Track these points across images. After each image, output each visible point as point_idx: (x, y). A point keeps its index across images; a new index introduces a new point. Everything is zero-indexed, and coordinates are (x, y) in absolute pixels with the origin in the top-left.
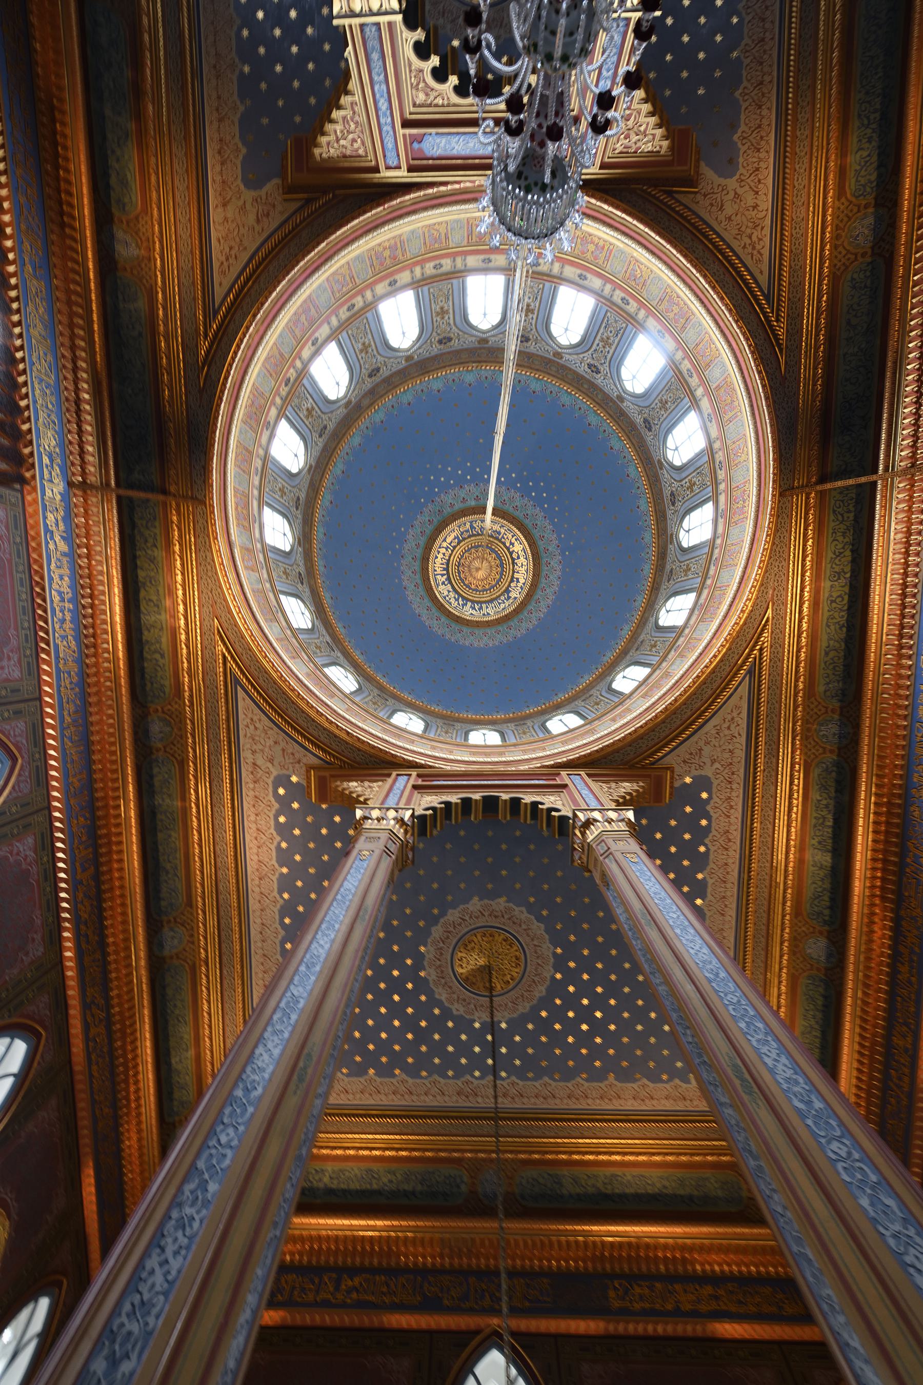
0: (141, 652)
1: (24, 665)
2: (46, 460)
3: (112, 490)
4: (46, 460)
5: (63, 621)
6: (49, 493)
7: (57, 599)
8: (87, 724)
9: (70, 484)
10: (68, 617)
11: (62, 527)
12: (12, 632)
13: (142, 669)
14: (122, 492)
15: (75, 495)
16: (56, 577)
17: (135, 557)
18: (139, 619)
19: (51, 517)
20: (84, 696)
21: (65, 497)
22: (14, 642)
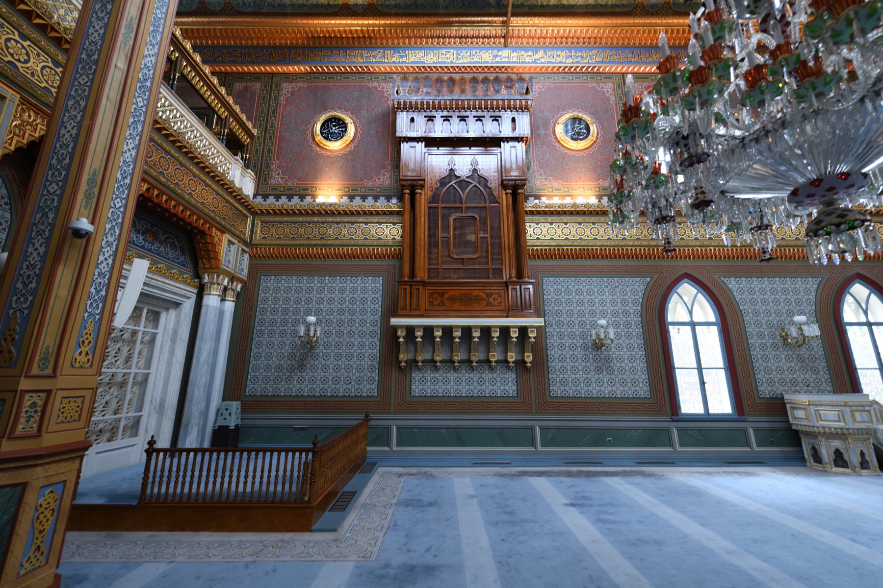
0: (601, 5)
1: (605, 80)
2: (498, 59)
3: (509, 20)
4: (498, 59)
5: (582, 57)
6: (515, 59)
7: (570, 60)
8: (640, 47)
9: (506, 46)
10: (579, 54)
11: (530, 53)
12: (589, 85)
13: (612, 5)
14: (509, 15)
15: (511, 43)
16: (559, 59)
17: (542, 6)
18: (581, 6)
19: (527, 60)
20: (624, 47)
21: (515, 49)
22: (594, 85)
